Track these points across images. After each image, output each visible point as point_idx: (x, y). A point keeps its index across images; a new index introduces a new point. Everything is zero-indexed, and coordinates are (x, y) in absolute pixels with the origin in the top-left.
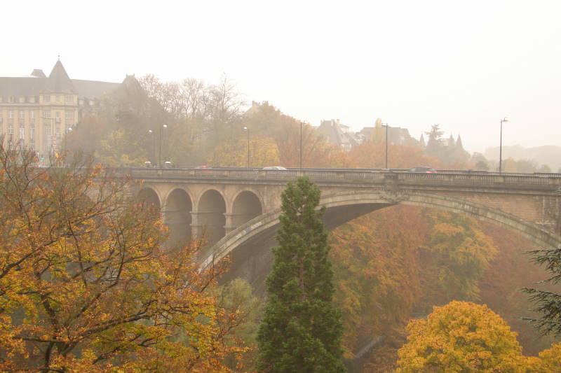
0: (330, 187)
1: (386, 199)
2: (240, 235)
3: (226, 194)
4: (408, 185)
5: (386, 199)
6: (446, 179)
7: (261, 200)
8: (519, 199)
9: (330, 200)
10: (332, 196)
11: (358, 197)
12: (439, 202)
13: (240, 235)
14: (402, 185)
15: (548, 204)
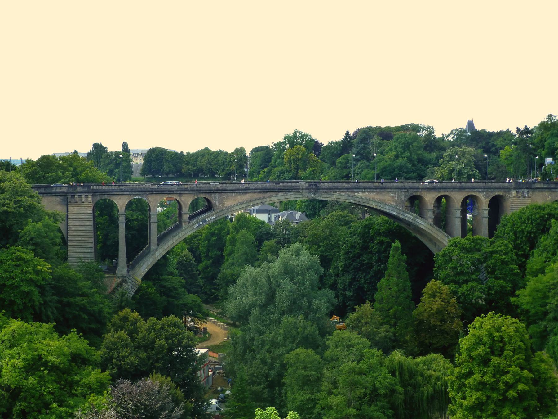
0: (267, 192)
1: (306, 197)
2: (197, 225)
3: (183, 200)
4: (324, 189)
5: (306, 197)
6: (346, 185)
7: (213, 201)
8: (384, 193)
9: (268, 199)
10: (270, 197)
11: (288, 197)
12: (340, 197)
13: (197, 225)
14: (319, 189)
15: (398, 195)
